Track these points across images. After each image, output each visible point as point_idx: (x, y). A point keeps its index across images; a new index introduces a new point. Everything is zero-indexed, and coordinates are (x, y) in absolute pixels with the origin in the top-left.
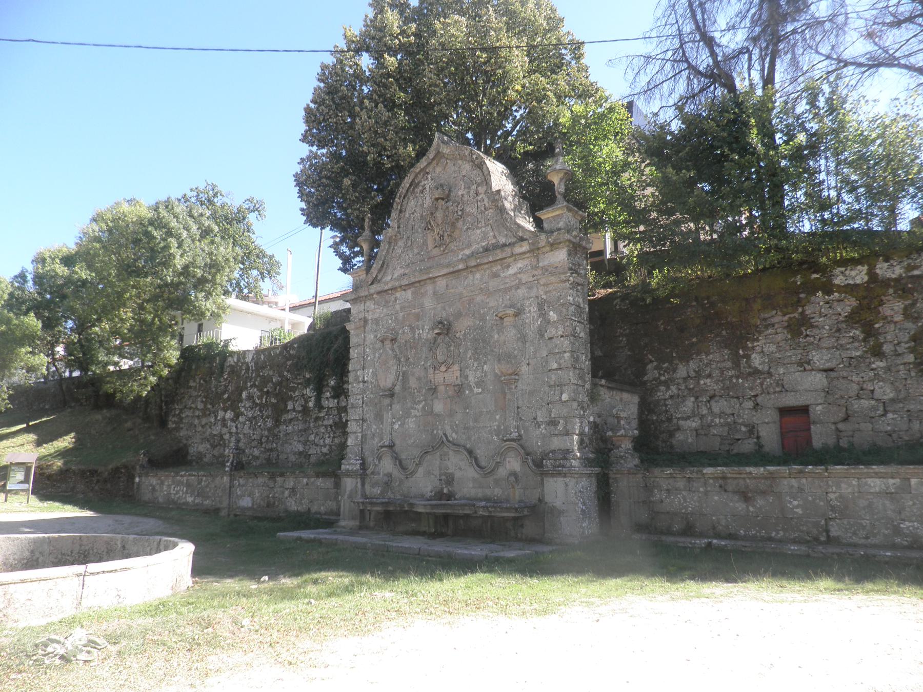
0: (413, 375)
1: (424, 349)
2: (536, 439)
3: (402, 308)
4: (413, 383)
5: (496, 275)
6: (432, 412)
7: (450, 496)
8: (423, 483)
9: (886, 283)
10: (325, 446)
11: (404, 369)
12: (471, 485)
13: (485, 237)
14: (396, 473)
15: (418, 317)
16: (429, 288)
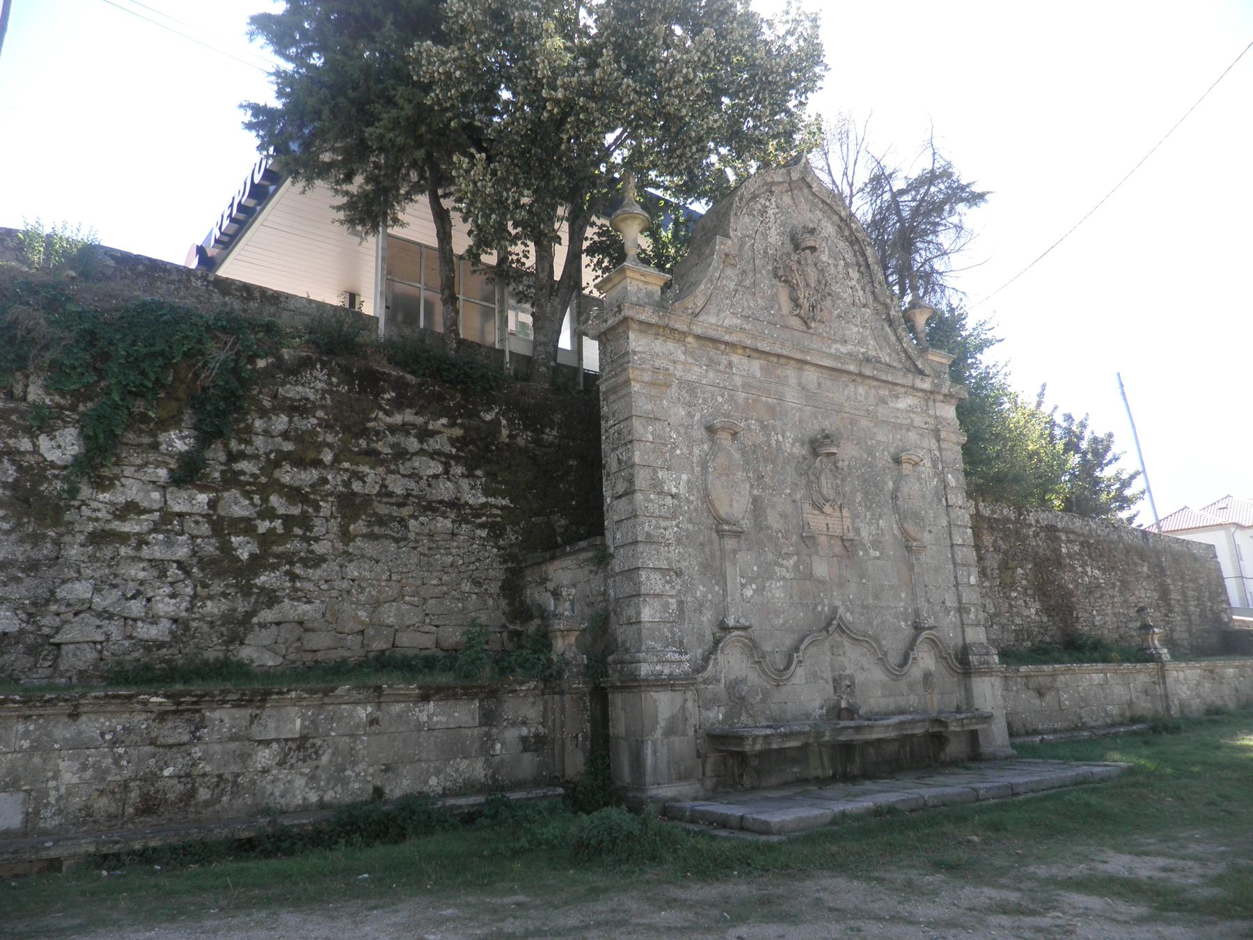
0: (773, 507)
1: (788, 467)
2: (948, 628)
3: (746, 386)
4: (773, 519)
5: (883, 401)
6: (811, 575)
7: (851, 712)
8: (806, 694)
9: (983, 517)
10: (154, 620)
11: (755, 492)
12: (879, 693)
13: (862, 342)
14: (754, 677)
15: (771, 410)
16: (791, 373)
